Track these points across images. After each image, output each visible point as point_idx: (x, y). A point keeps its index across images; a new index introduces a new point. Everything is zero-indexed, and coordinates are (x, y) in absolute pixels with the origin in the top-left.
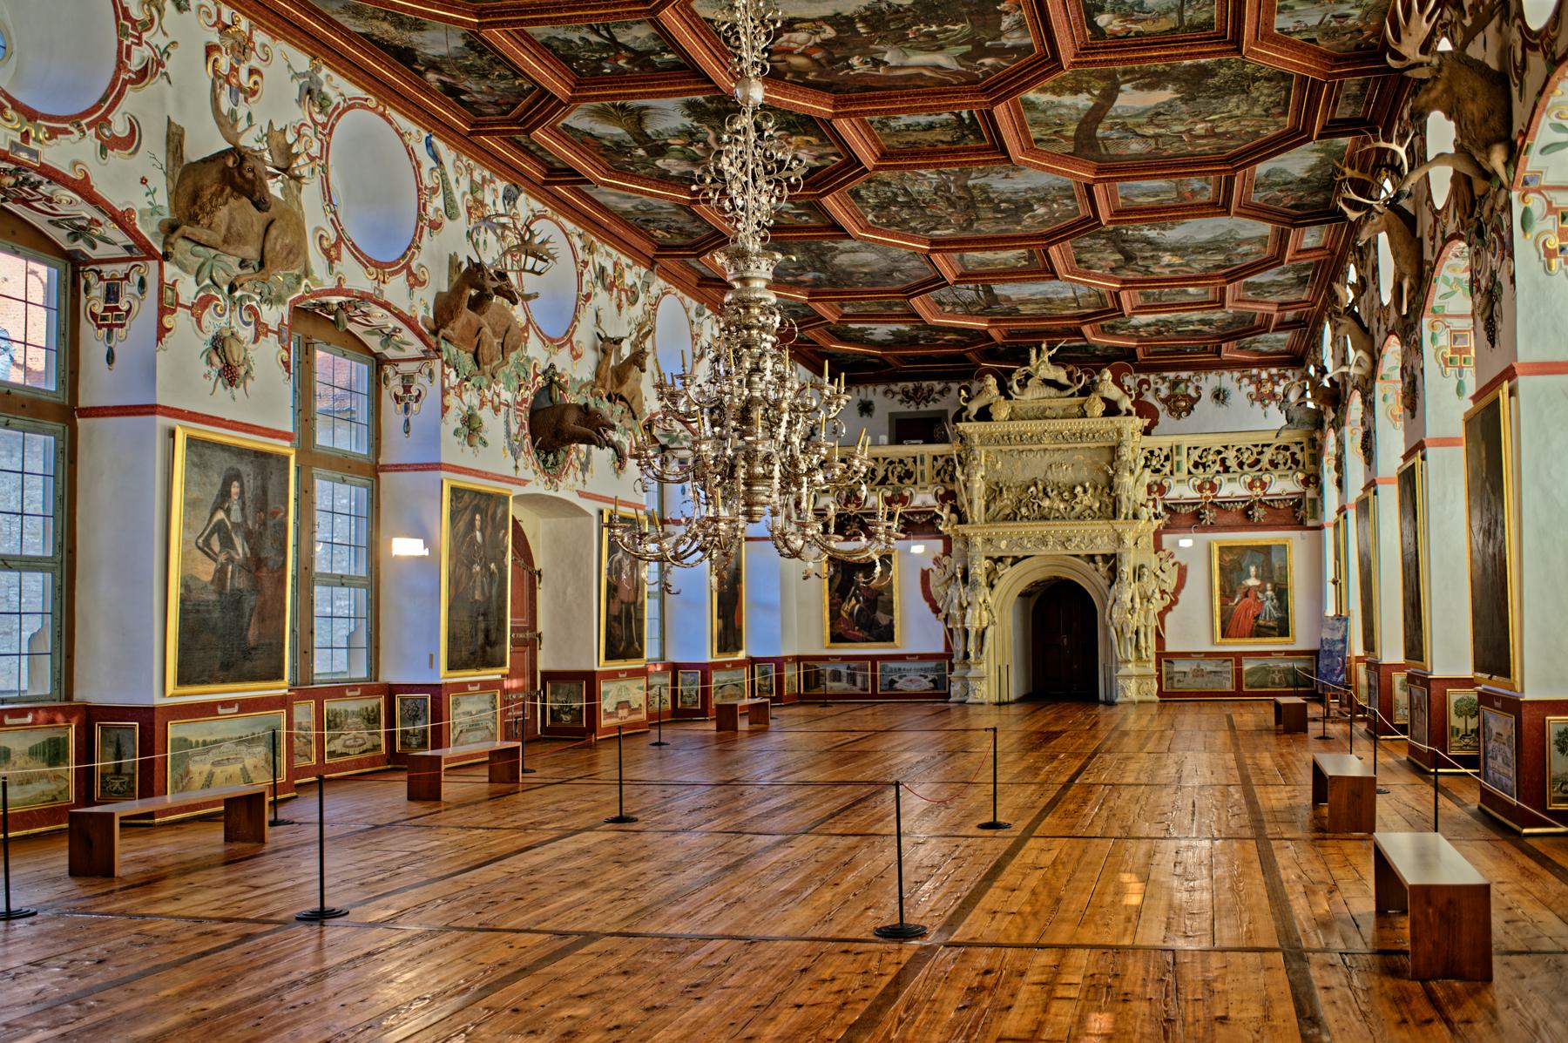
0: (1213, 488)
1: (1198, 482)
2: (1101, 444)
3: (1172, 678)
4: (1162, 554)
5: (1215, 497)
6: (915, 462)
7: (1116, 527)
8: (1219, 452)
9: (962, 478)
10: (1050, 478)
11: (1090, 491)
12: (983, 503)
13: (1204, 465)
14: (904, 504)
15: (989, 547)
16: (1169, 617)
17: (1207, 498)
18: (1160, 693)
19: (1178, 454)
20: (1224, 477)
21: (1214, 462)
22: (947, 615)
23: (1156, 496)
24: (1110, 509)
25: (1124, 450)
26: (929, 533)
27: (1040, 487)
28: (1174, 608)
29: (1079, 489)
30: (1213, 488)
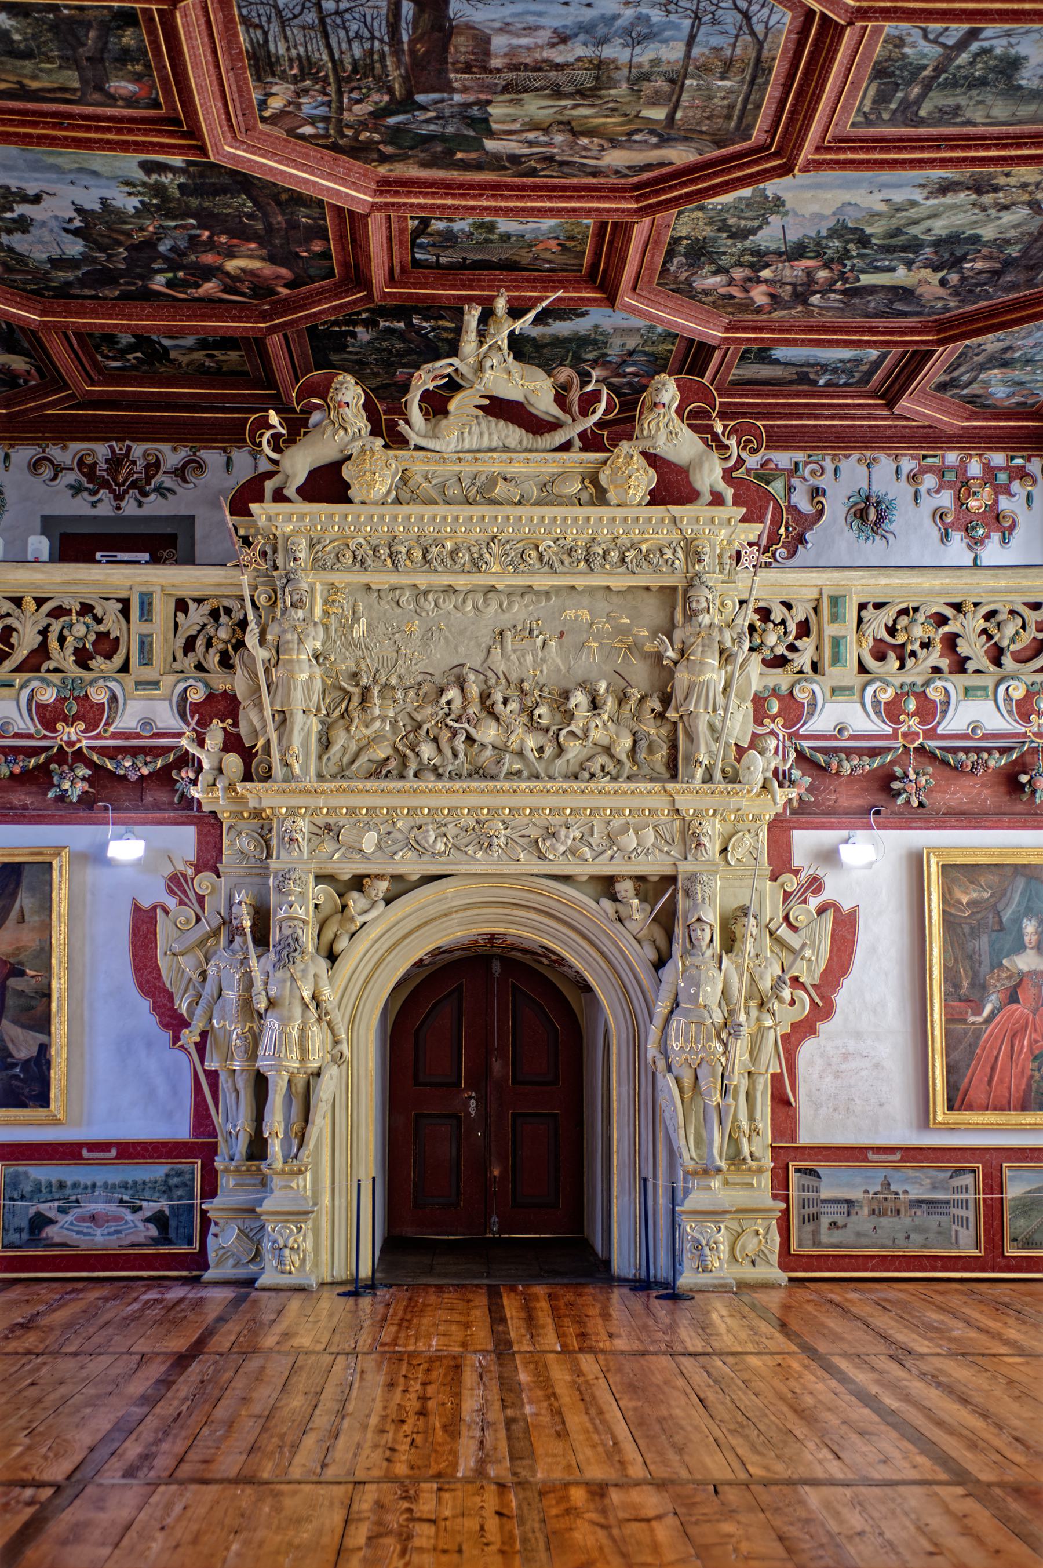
0: (927, 711)
1: (887, 695)
2: (641, 581)
3: (815, 1218)
4: (790, 882)
5: (931, 734)
6: (125, 612)
7: (681, 801)
8: (941, 620)
9: (261, 654)
10: (501, 667)
11: (610, 704)
12: (316, 727)
13: (900, 650)
14: (91, 726)
15: (329, 847)
16: (807, 1049)
17: (909, 735)
19: (835, 618)
20: (954, 684)
21: (926, 645)
22: (204, 1035)
23: (778, 726)
24: (664, 751)
25: (702, 597)
26: (157, 807)
27: (474, 690)
28: (823, 1027)
29: (579, 698)
30: (927, 711)
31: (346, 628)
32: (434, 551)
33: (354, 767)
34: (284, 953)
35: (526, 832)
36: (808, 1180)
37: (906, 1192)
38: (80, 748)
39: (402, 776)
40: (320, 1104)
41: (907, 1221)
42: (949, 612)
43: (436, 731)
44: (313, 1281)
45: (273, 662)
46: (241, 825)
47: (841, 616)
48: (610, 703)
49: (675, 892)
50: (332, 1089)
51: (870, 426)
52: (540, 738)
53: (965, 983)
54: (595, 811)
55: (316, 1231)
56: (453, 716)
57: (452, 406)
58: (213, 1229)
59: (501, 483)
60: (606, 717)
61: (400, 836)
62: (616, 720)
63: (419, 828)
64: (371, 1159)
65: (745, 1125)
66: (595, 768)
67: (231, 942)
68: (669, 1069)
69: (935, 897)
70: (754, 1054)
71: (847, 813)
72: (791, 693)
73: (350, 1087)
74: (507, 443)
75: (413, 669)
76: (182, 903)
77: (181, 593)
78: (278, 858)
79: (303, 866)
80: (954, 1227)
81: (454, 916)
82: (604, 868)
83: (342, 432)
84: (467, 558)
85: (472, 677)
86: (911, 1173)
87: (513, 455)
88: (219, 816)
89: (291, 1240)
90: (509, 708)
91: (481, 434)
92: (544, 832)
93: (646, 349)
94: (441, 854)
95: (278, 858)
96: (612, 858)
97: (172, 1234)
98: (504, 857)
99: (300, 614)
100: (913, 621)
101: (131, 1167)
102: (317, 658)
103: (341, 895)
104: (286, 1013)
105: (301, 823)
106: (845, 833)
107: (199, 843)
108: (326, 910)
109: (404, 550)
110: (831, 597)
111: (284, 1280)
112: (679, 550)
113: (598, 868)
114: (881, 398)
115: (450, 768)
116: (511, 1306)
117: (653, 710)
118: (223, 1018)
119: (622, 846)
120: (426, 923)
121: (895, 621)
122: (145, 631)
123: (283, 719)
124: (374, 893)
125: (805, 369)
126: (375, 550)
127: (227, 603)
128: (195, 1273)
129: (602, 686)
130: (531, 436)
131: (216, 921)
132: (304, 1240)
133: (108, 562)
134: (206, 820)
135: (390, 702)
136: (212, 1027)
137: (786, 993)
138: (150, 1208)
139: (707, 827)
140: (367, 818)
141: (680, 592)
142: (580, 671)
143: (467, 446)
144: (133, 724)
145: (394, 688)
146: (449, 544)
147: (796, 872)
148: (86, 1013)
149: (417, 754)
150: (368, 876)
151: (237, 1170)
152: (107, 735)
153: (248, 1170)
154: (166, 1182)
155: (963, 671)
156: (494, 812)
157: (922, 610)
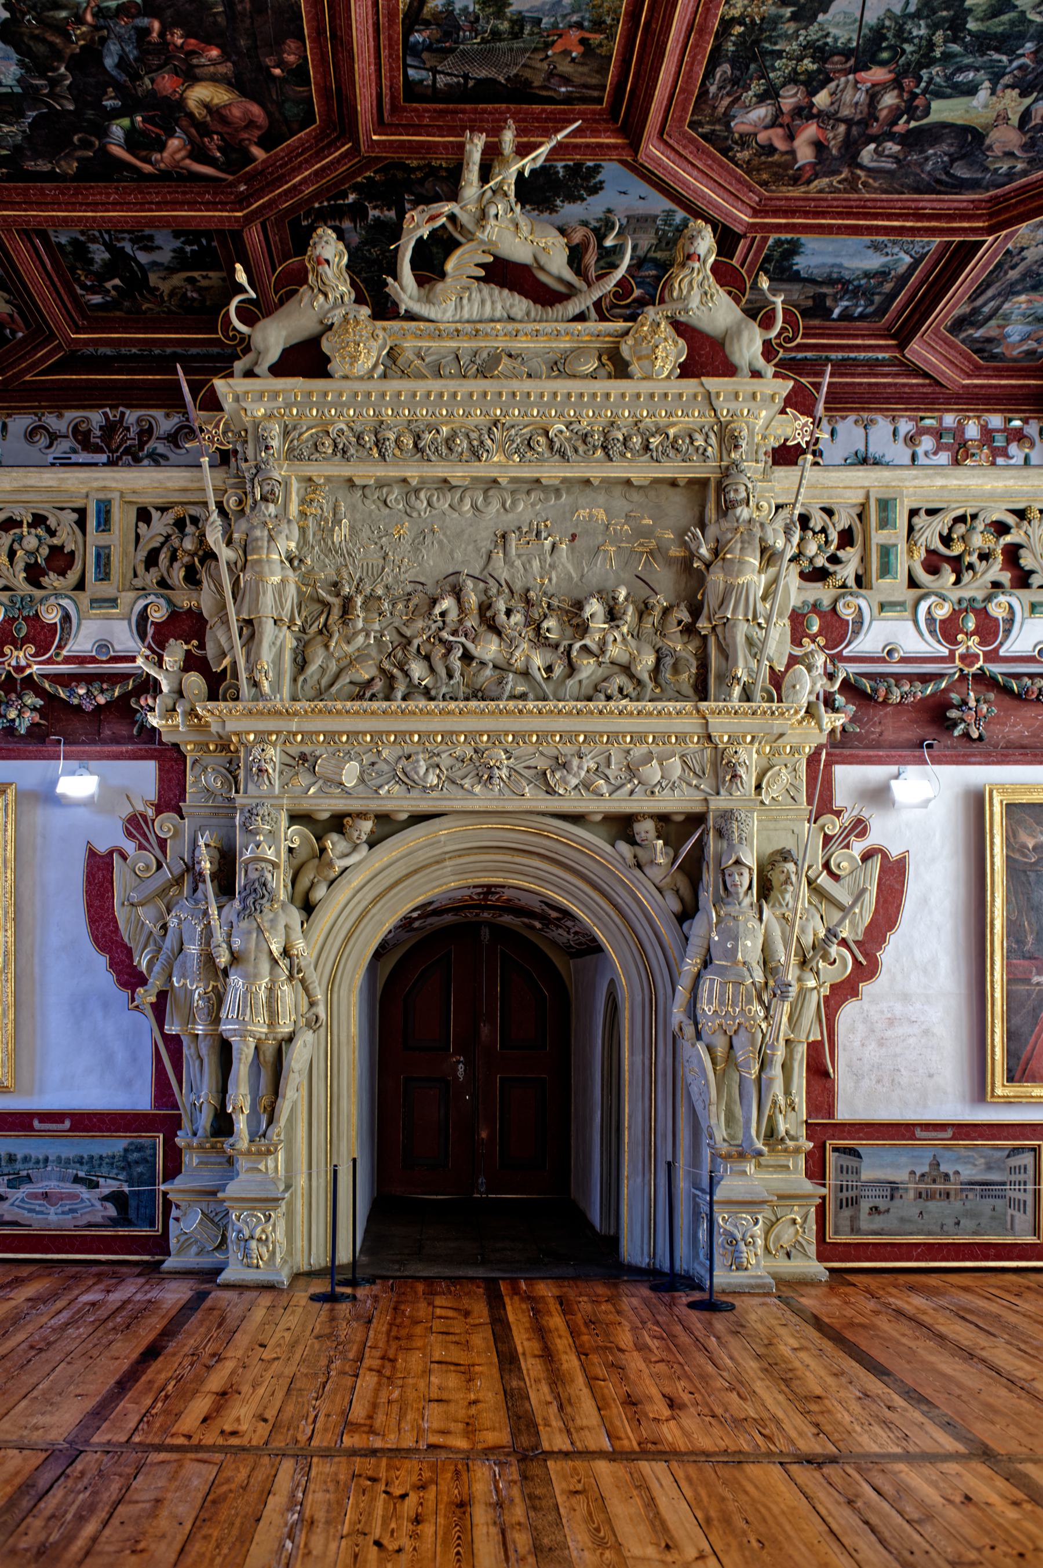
1: (942, 612)
3: (854, 1202)
4: (833, 826)
5: (992, 657)
8: (1001, 528)
9: (225, 554)
10: (504, 575)
12: (290, 643)
13: (957, 564)
15: (303, 779)
16: (848, 1013)
17: (969, 658)
18: (825, 1251)
20: (1016, 600)
21: (984, 557)
22: (162, 995)
27: (473, 600)
29: (594, 607)
31: (326, 531)
32: (428, 437)
33: (334, 689)
34: (250, 901)
36: (847, 1161)
37: (957, 1173)
38: (31, 674)
39: (387, 698)
40: (292, 1075)
41: (958, 1204)
42: (1011, 520)
44: (284, 1277)
46: (207, 759)
47: (891, 521)
48: (631, 609)
49: (705, 833)
50: (306, 1057)
51: (870, 384)
53: (1030, 939)
54: (614, 737)
55: (290, 1216)
56: (448, 629)
57: (450, 266)
58: (174, 1213)
59: (505, 360)
60: (625, 629)
61: (385, 768)
62: (637, 636)
63: (408, 757)
64: (354, 1133)
65: (781, 1100)
66: (612, 689)
67: (195, 890)
68: (699, 1036)
69: (997, 840)
70: (794, 1022)
71: (893, 746)
72: (834, 610)
73: (331, 1056)
75: (402, 577)
76: (141, 847)
77: (145, 500)
78: (245, 792)
79: (273, 801)
80: (1010, 1211)
81: (447, 863)
82: (623, 804)
85: (470, 584)
86: (964, 1153)
87: (519, 326)
88: (182, 748)
89: (259, 1229)
91: (483, 302)
92: (553, 762)
93: (658, 255)
94: (433, 788)
95: (245, 792)
96: (632, 792)
97: (132, 1215)
98: (506, 791)
99: (272, 509)
100: (972, 529)
101: (88, 1140)
102: (291, 561)
103: (319, 839)
104: (251, 969)
105: (271, 752)
106: (893, 769)
107: (161, 780)
108: (302, 855)
109: (392, 437)
110: (879, 501)
111: (250, 1276)
112: (712, 435)
113: (616, 804)
114: (892, 337)
115: (444, 690)
116: (516, 1314)
117: (680, 622)
118: (184, 976)
119: (644, 778)
120: (415, 872)
121: (950, 529)
122: (102, 543)
123: (250, 628)
124: (356, 834)
125: (825, 290)
126: (359, 437)
127: (193, 511)
128: (157, 1258)
129: (622, 593)
130: (539, 307)
131: (179, 867)
132: (274, 1230)
133: (62, 465)
134: (169, 754)
135: (376, 615)
136: (172, 985)
137: (834, 950)
138: (108, 1186)
139: (743, 756)
140: (347, 747)
141: (713, 485)
143: (466, 316)
144: (88, 647)
145: (379, 598)
146: (445, 430)
147: (838, 813)
148: (37, 970)
149: (407, 674)
150: (349, 815)
151: (201, 1147)
152: (59, 659)
153: (212, 1147)
154: (124, 1158)
155: (1026, 585)
156: (496, 737)
157: (981, 517)
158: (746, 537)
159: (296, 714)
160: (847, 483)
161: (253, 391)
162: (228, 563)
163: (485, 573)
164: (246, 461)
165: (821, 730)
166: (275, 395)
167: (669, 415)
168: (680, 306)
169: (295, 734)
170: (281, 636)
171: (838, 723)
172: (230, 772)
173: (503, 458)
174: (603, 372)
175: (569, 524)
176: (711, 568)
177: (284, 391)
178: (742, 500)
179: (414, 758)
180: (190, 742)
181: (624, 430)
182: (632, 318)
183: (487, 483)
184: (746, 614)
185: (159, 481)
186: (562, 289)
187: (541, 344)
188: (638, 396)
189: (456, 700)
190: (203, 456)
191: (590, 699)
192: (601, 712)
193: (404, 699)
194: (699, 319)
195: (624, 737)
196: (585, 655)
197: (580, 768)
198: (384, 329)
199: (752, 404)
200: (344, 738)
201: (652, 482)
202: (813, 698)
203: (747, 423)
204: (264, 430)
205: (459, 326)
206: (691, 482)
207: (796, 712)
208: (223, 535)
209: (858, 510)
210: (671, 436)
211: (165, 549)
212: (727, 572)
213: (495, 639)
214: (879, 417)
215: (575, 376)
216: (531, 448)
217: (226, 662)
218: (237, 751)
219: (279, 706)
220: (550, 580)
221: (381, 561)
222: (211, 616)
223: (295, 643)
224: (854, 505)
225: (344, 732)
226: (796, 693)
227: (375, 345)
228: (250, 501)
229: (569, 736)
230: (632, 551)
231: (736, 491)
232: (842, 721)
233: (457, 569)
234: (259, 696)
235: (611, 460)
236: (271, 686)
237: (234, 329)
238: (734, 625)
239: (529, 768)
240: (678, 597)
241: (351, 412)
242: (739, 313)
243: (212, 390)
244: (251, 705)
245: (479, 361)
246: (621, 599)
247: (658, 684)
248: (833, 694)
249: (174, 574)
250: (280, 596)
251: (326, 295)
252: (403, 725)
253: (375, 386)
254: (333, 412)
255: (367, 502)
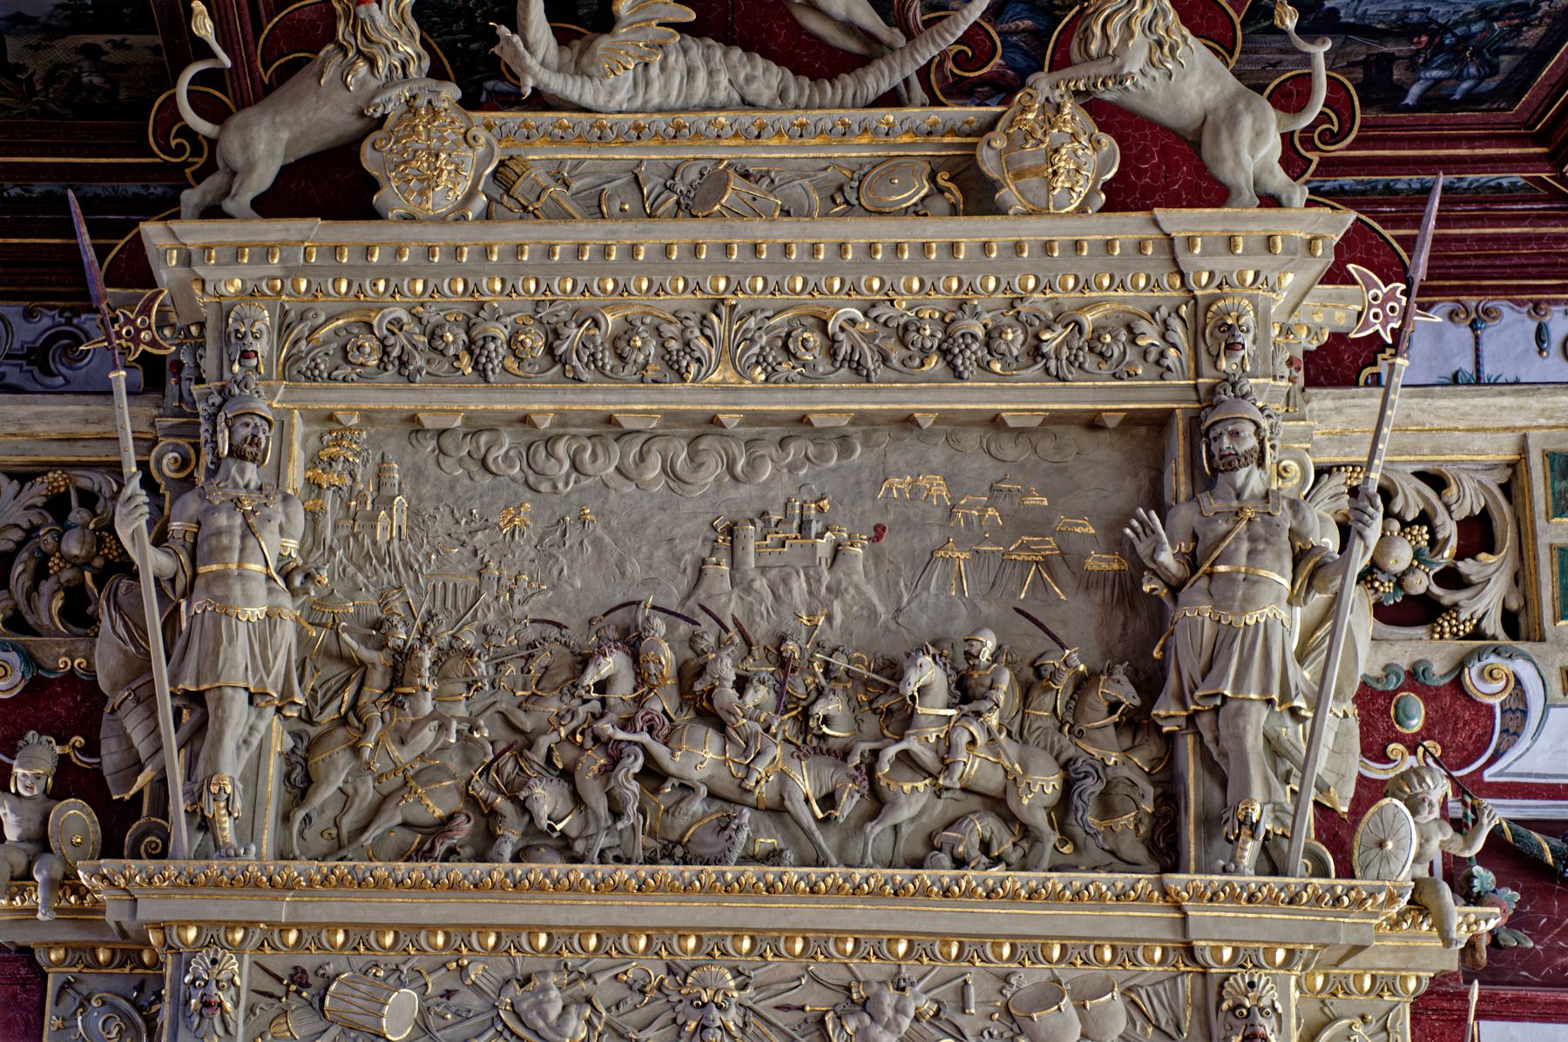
9: (153, 562)
10: (732, 608)
12: (280, 742)
27: (666, 657)
31: (358, 519)
32: (574, 334)
33: (368, 838)
35: (792, 998)
39: (480, 857)
43: (570, 752)
45: (181, 583)
52: (827, 772)
56: (612, 716)
61: (475, 1003)
66: (968, 845)
72: (1458, 684)
74: (752, 91)
75: (517, 612)
83: (362, 67)
84: (652, 349)
85: (659, 624)
87: (765, 117)
90: (751, 698)
91: (691, 72)
99: (252, 473)
102: (287, 578)
109: (502, 334)
115: (602, 841)
126: (434, 335)
130: (806, 81)
135: (460, 687)
142: (924, 622)
143: (656, 98)
145: (469, 653)
146: (610, 320)
149: (523, 808)
156: (714, 942)
158: (1260, 530)
159: (289, 886)
160: (1476, 421)
161: (221, 244)
162: (157, 579)
163: (691, 603)
164: (200, 380)
165: (1447, 941)
166: (267, 251)
167: (1083, 285)
168: (1105, 69)
169: (284, 929)
170: (262, 727)
171: (1484, 928)
172: (140, 1009)
173: (731, 377)
174: (939, 203)
175: (868, 505)
176: (1182, 596)
177: (283, 244)
178: (1247, 454)
179: (536, 982)
180: (58, 945)
181: (987, 318)
182: (1006, 101)
183: (695, 424)
184: (1265, 689)
185: (19, 422)
186: (853, 45)
187: (811, 152)
188: (1018, 247)
189: (629, 861)
190: (115, 368)
191: (918, 864)
192: (946, 892)
193: (516, 858)
194: (1146, 95)
195: (997, 946)
196: (906, 772)
197: (899, 1010)
198: (489, 127)
199: (1265, 261)
200: (389, 940)
201: (1046, 422)
202: (1423, 872)
203: (1253, 300)
204: (240, 319)
205: (642, 119)
206: (1133, 420)
207: (1392, 899)
208: (150, 523)
209: (1502, 476)
210: (1088, 328)
211: (24, 555)
212: (1220, 602)
213: (713, 737)
214: (1503, 305)
215: (881, 213)
216: (792, 355)
217: (142, 780)
218: (157, 964)
219: (253, 868)
220: (829, 618)
221: (473, 581)
222: (115, 688)
223: (290, 743)
224: (1492, 467)
225: (389, 926)
226: (1386, 859)
227: (469, 157)
228: (206, 459)
229: (874, 943)
230: (1004, 560)
231: (1235, 434)
232: (1492, 924)
233: (632, 596)
234: (211, 846)
235: (959, 377)
236: (237, 829)
237: (188, 132)
238: (1239, 713)
239: (786, 1008)
240: (1108, 653)
241: (419, 286)
242: (1232, 83)
243: (138, 244)
244: (194, 866)
245: (680, 187)
246: (985, 656)
247: (1066, 836)
248: (1465, 862)
249: (42, 604)
250: (264, 647)
251: (372, 63)
252: (514, 912)
253: (468, 235)
254: (381, 285)
255: (447, 463)
